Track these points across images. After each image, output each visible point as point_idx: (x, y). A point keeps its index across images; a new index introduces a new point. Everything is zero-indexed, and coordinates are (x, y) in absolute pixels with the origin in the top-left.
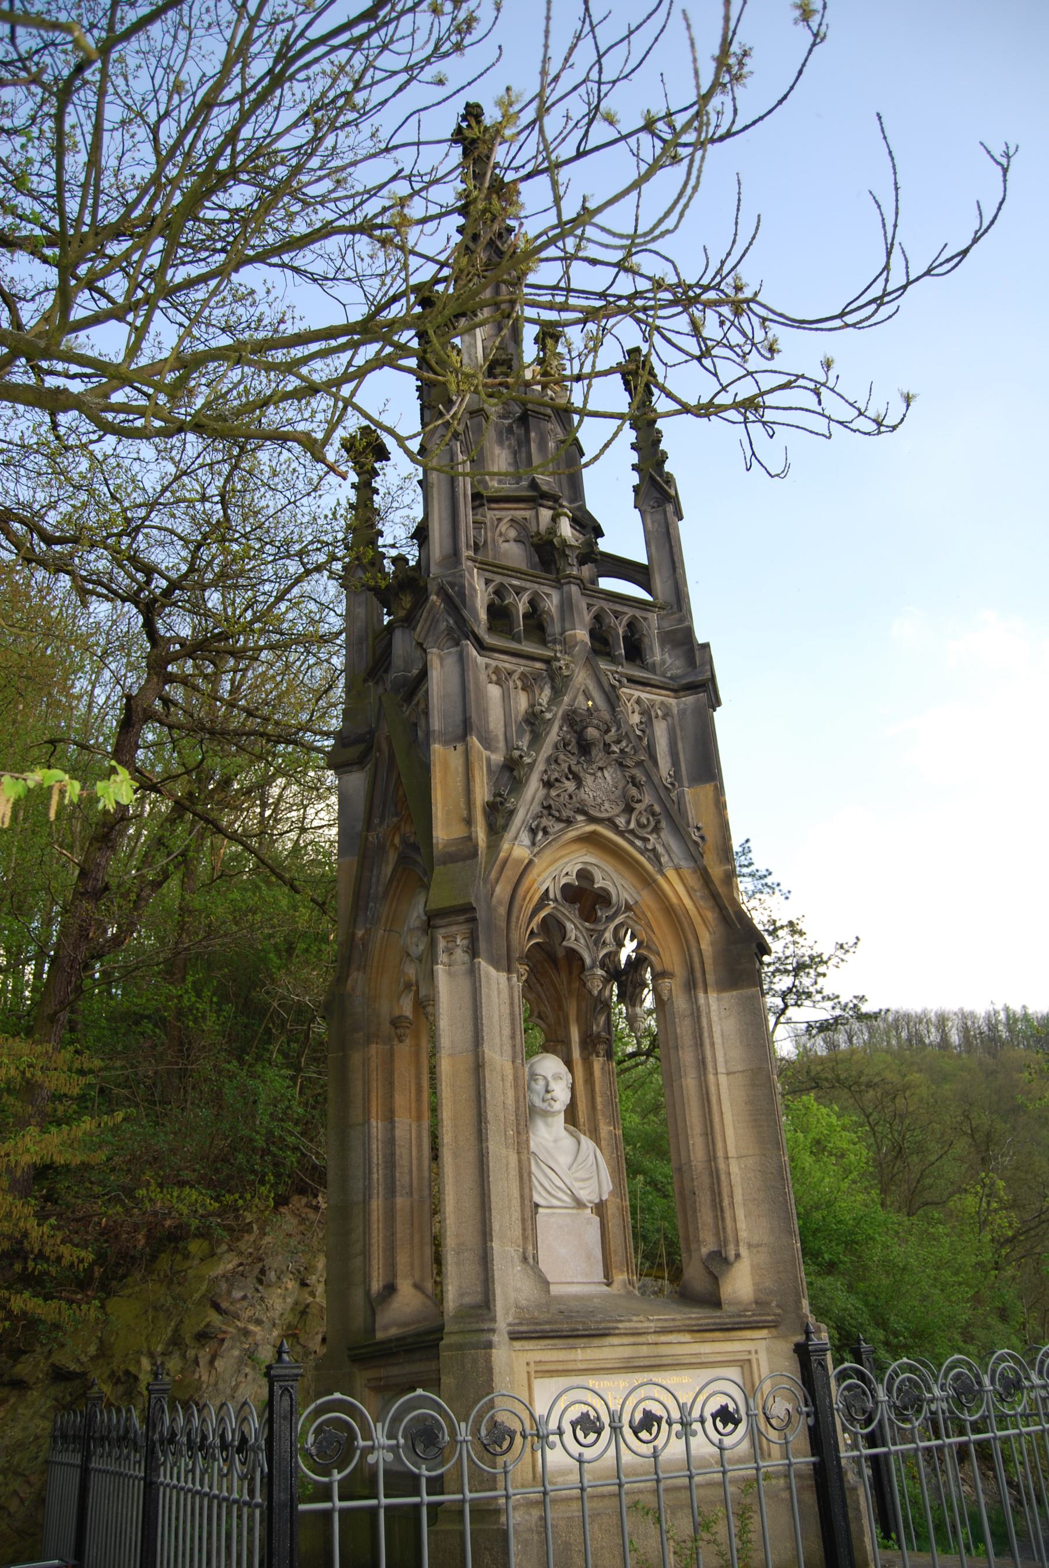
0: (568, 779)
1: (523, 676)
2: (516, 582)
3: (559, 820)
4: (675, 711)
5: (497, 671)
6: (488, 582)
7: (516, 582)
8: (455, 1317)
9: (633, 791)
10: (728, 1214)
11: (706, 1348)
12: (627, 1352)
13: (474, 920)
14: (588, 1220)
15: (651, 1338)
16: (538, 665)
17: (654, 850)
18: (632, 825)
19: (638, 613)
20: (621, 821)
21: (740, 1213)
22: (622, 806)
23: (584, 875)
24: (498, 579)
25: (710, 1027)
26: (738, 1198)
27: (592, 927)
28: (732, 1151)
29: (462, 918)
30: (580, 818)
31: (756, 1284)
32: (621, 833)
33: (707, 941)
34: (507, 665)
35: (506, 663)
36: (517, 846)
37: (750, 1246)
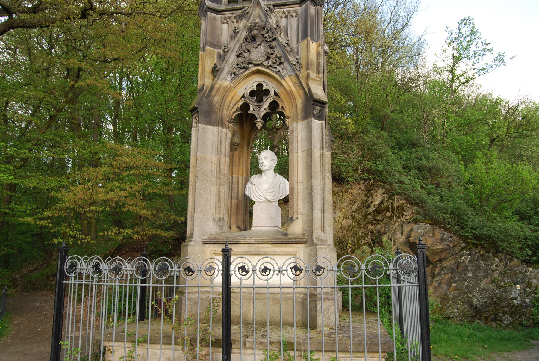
0: (245, 52)
1: (235, 18)
3: (241, 68)
4: (299, 12)
5: (225, 19)
8: (189, 237)
9: (270, 51)
10: (295, 203)
11: (276, 249)
12: (247, 249)
13: (198, 112)
15: (255, 245)
16: (240, 11)
17: (279, 71)
18: (269, 64)
20: (266, 63)
21: (300, 203)
22: (266, 57)
23: (260, 86)
26: (300, 197)
27: (258, 104)
28: (300, 180)
29: (195, 112)
30: (251, 65)
31: (303, 228)
32: (268, 67)
33: (300, 102)
34: (229, 15)
35: (228, 14)
36: (225, 81)
37: (302, 214)
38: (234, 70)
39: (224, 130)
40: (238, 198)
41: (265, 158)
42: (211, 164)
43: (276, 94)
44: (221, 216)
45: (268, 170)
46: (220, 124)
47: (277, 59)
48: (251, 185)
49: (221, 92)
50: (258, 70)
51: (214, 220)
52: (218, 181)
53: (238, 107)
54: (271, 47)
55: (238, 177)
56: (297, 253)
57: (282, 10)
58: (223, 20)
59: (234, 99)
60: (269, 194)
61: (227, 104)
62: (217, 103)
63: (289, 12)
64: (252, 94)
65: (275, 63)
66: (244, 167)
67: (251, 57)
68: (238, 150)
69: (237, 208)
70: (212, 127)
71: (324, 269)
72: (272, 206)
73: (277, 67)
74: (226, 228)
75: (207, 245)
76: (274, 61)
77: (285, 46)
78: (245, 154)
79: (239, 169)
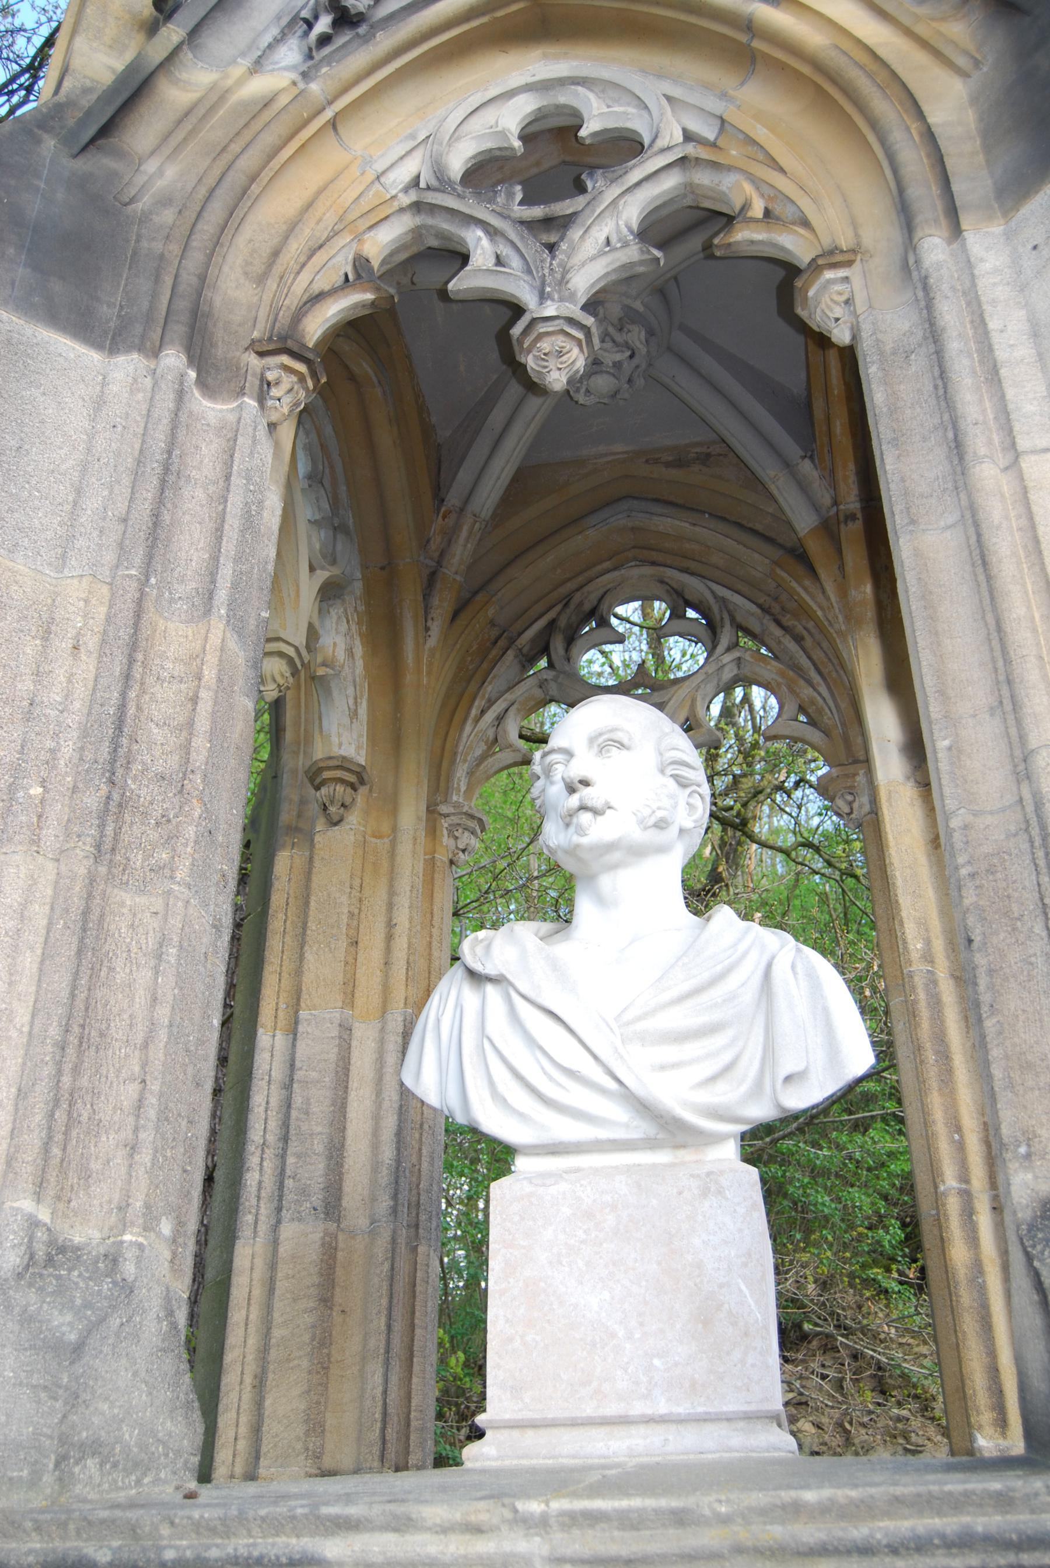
14: (710, 1185)
25: (980, 322)
27: (537, 212)
40: (332, 1207)
41: (607, 743)
42: (31, 648)
44: (86, 1234)
45: (638, 852)
46: (179, 329)
48: (470, 996)
49: (214, 132)
52: (92, 800)
55: (346, 1030)
59: (320, 207)
60: (670, 1053)
62: (165, 201)
64: (486, 172)
66: (401, 943)
68: (353, 819)
69: (326, 1301)
70: (93, 357)
72: (710, 1185)
74: (138, 1390)
78: (405, 849)
79: (351, 964)
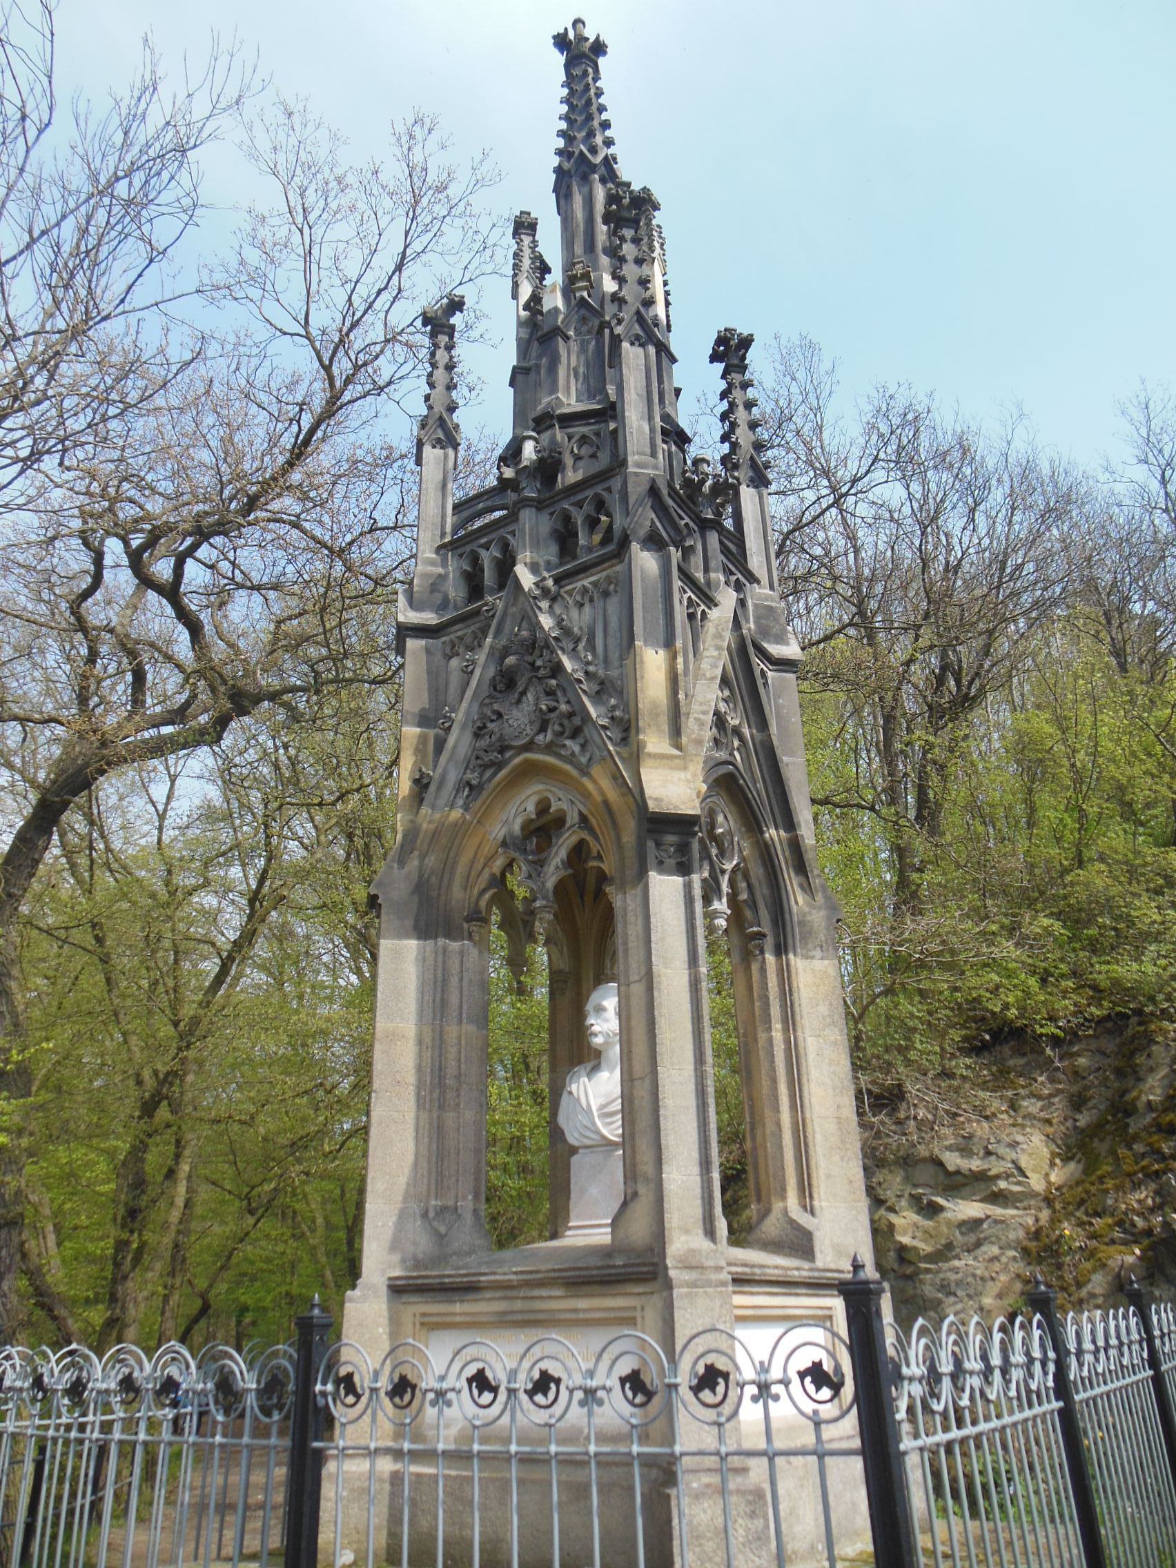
2: (483, 541)
6: (461, 556)
7: (483, 541)
11: (583, 1304)
12: (501, 1306)
17: (573, 754)
19: (599, 489)
24: (468, 548)
30: (508, 755)
32: (549, 748)
38: (469, 776)
39: (455, 945)
43: (583, 819)
47: (566, 722)
50: (526, 761)
51: (425, 1215)
52: (435, 1095)
53: (493, 875)
54: (550, 693)
56: (638, 1314)
57: (579, 584)
58: (448, 650)
61: (461, 870)
63: (594, 584)
65: (562, 734)
67: (508, 731)
71: (558, 1381)
73: (568, 742)
75: (405, 1298)
76: (557, 728)
77: (580, 681)
